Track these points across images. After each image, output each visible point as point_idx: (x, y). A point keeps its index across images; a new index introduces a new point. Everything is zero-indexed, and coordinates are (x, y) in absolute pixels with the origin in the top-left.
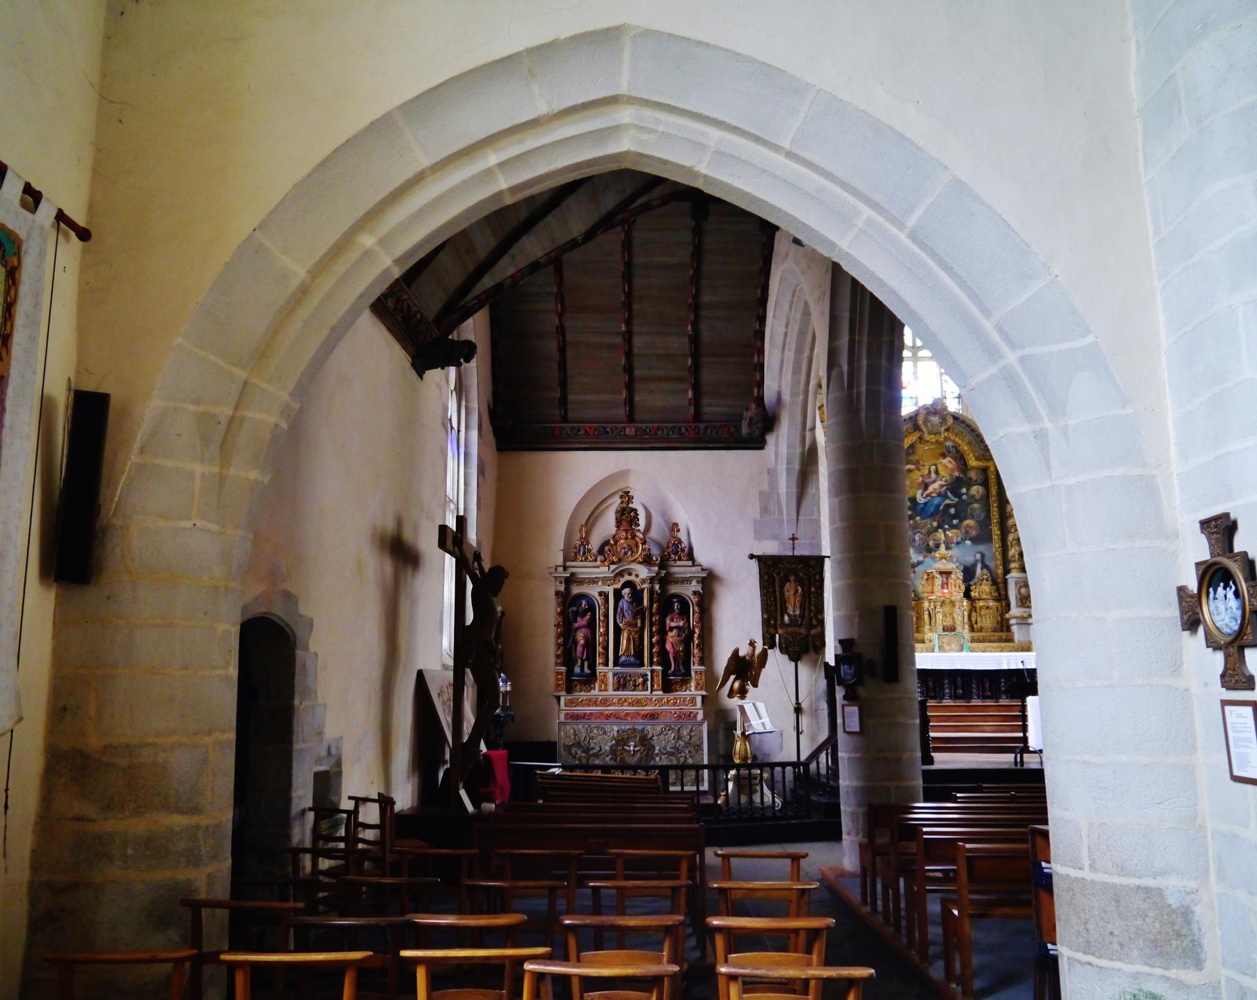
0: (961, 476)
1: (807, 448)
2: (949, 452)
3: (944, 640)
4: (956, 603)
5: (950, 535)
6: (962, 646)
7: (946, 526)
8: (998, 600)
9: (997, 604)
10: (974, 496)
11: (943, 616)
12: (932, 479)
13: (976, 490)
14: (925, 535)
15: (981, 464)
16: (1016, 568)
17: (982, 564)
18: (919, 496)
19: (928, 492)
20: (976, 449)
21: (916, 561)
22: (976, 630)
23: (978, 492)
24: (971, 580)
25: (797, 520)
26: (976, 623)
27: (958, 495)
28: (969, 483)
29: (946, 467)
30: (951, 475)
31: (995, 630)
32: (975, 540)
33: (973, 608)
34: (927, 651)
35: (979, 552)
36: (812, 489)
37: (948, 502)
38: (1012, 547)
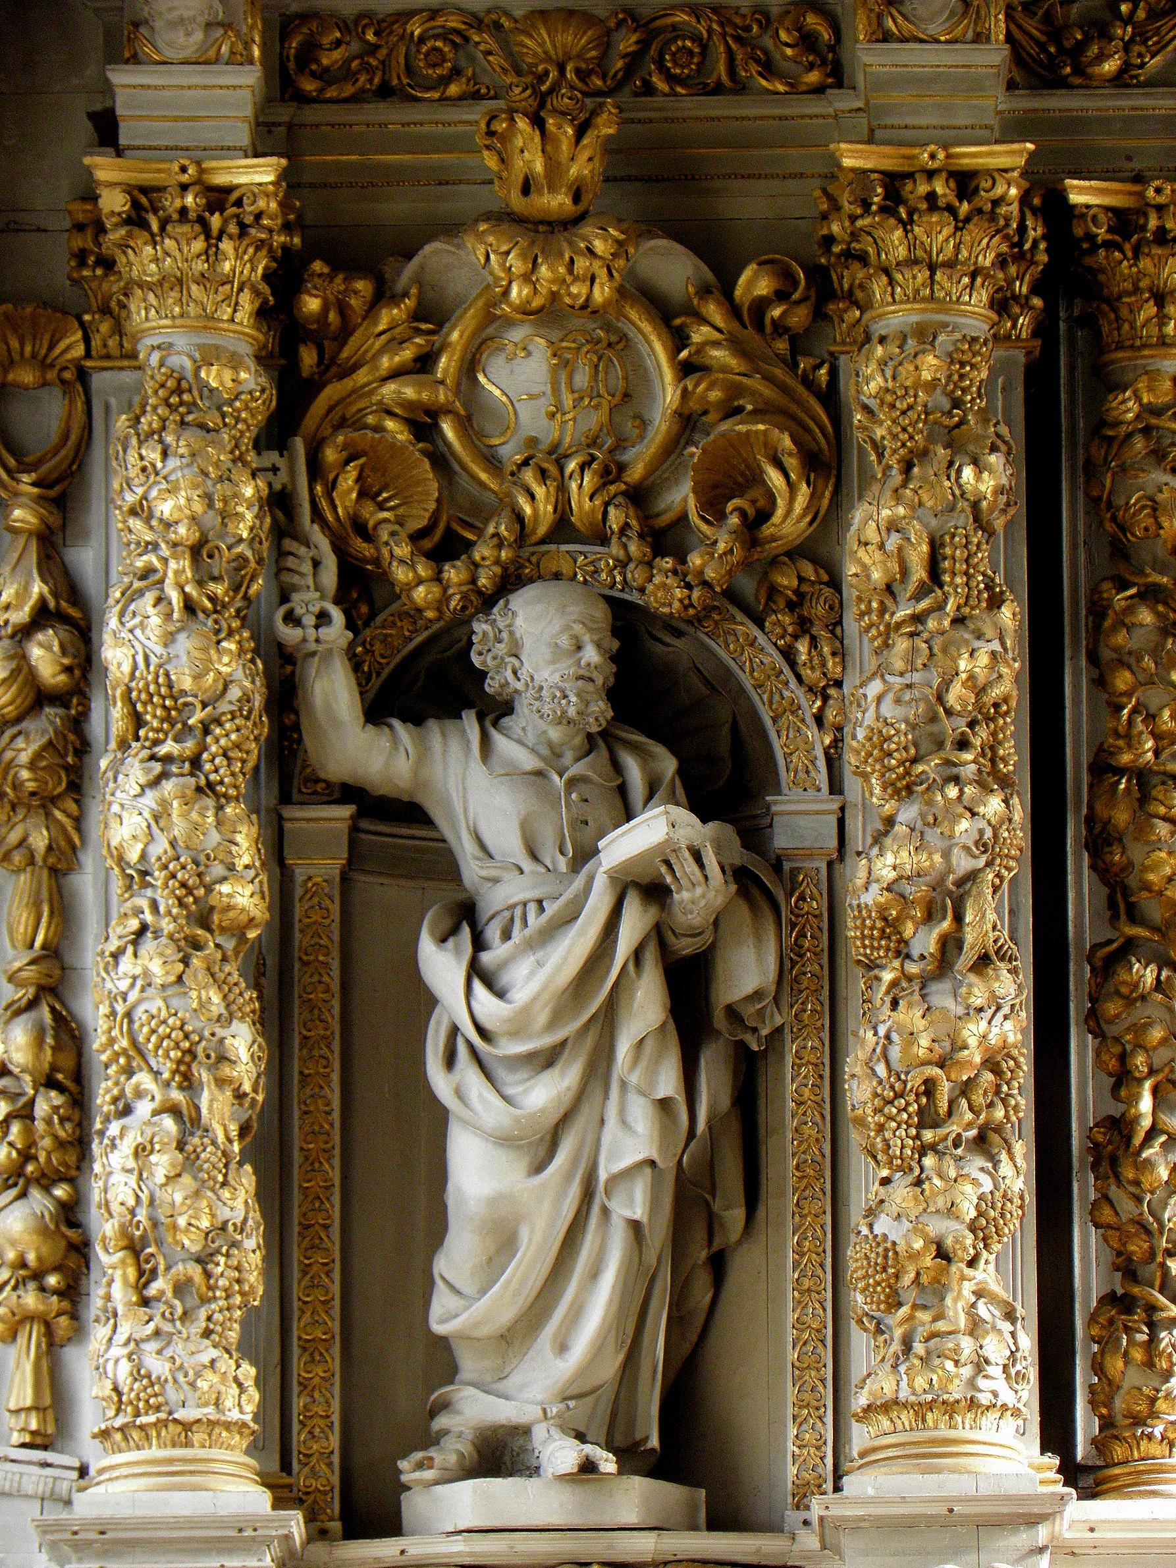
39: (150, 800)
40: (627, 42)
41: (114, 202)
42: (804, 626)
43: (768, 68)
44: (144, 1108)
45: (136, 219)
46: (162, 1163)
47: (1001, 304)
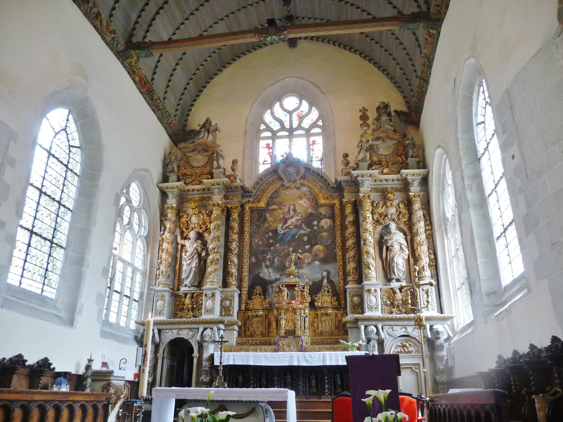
0: (313, 212)
2: (305, 195)
5: (300, 256)
7: (300, 251)
9: (336, 312)
11: (286, 322)
12: (291, 216)
14: (282, 258)
18: (279, 228)
19: (287, 225)
20: (326, 192)
21: (274, 278)
23: (327, 224)
26: (318, 329)
28: (319, 217)
29: (302, 206)
30: (306, 212)
35: (326, 271)
37: (302, 232)
38: (349, 263)
46: (163, 267)
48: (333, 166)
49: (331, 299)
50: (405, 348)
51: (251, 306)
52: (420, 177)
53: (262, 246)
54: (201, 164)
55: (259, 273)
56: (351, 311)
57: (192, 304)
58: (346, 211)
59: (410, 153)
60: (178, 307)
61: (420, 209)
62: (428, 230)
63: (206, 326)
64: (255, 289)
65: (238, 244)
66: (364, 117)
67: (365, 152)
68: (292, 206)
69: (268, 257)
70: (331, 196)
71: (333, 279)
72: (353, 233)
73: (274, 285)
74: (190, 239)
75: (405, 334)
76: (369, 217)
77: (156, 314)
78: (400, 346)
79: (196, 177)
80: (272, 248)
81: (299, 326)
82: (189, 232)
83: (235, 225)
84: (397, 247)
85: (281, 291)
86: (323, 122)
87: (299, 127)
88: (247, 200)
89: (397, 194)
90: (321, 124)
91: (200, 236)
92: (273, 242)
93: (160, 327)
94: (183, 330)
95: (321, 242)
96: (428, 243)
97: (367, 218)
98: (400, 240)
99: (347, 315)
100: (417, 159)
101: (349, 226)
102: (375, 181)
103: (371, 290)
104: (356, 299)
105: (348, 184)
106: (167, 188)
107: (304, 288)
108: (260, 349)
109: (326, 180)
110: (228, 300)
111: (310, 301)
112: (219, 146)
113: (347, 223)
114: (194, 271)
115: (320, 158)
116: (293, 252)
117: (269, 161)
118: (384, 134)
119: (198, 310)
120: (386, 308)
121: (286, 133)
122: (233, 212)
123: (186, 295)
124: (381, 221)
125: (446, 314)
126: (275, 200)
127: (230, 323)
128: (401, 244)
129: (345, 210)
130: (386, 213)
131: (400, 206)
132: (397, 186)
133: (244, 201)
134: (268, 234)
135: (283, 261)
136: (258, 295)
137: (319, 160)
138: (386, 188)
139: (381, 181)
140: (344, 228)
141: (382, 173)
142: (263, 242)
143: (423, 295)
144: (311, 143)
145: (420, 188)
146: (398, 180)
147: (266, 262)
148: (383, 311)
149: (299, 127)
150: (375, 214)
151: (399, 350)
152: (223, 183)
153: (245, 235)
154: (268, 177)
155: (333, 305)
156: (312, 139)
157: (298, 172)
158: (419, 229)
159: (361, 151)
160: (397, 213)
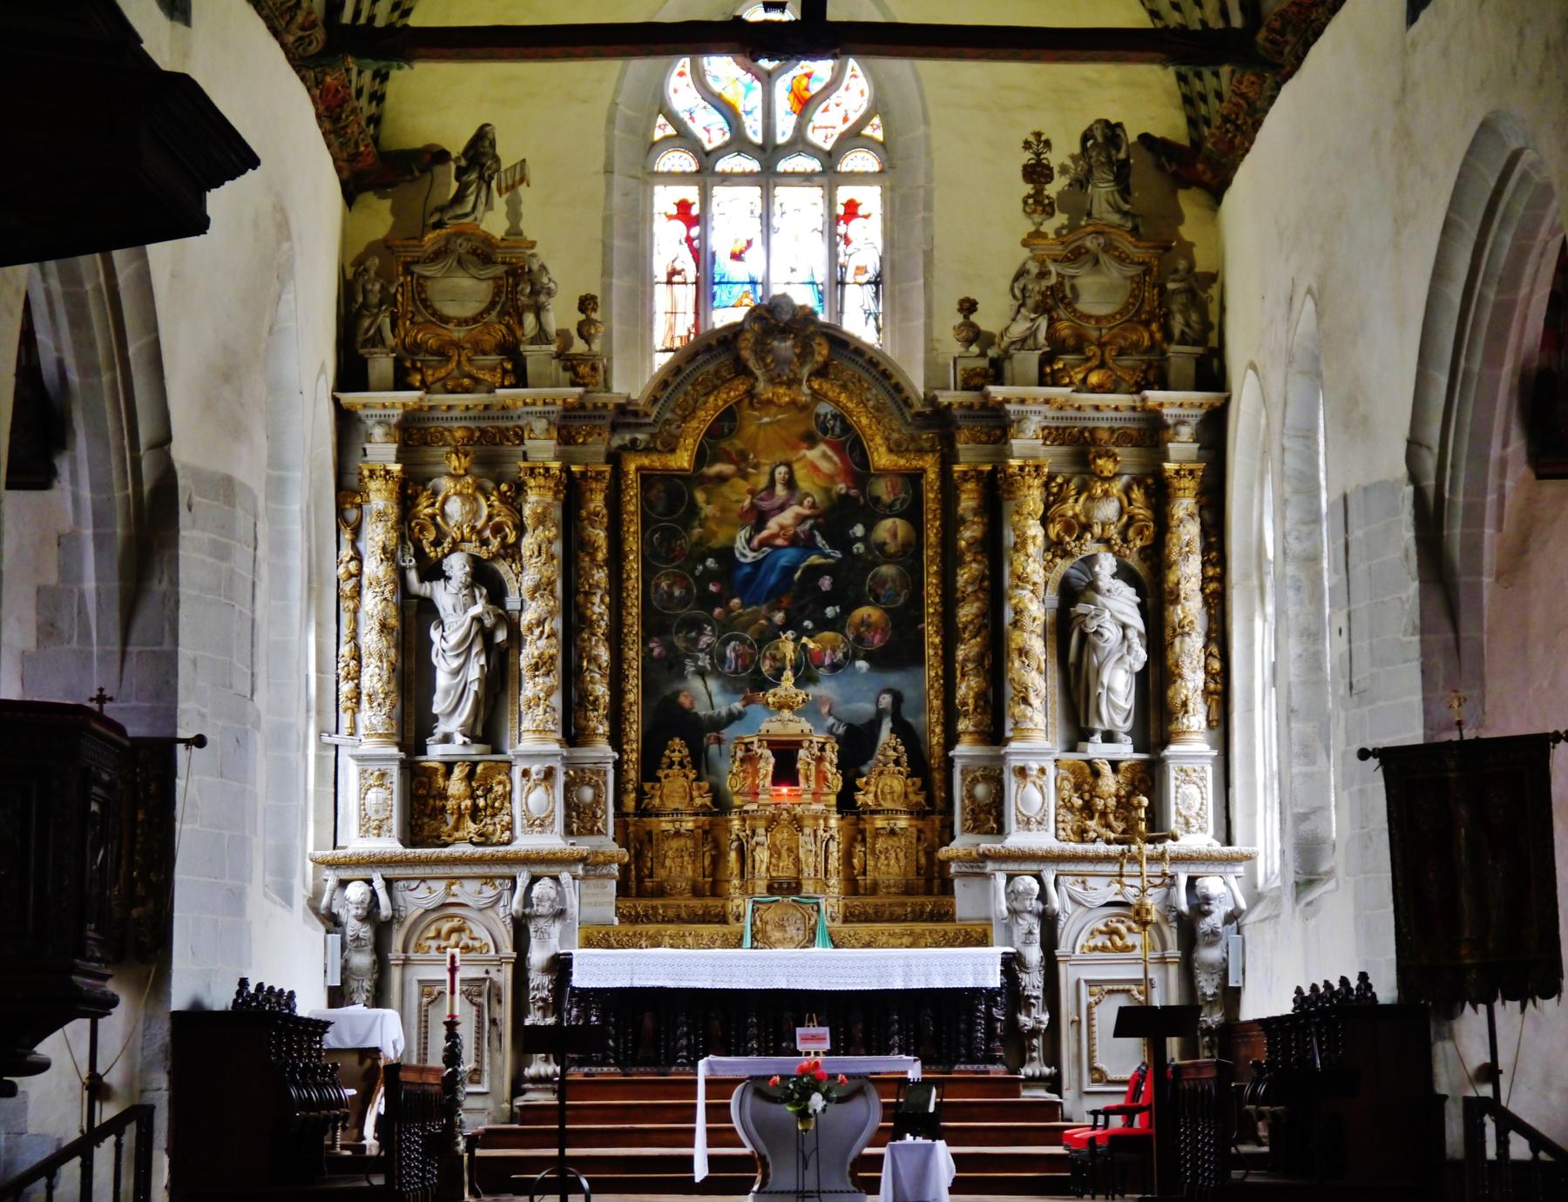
0: (853, 492)
1: (146, 488)
2: (825, 431)
3: (768, 916)
4: (806, 822)
5: (811, 645)
6: (813, 931)
7: (808, 624)
8: (916, 813)
9: (920, 824)
10: (885, 544)
11: (771, 856)
12: (777, 502)
13: (890, 530)
14: (751, 646)
15: (902, 462)
16: (970, 733)
17: (893, 721)
18: (740, 544)
19: (765, 533)
20: (896, 424)
21: (724, 712)
22: (862, 891)
23: (895, 535)
24: (864, 762)
25: (124, 654)
26: (864, 873)
27: (841, 540)
28: (872, 512)
29: (815, 468)
30: (827, 491)
31: (908, 890)
32: (882, 660)
33: (856, 836)
34: (726, 944)
36: (160, 582)
37: (814, 559)
38: (963, 675)
39: (373, 602)
40: (477, 434)
41: (366, 473)
42: (514, 561)
43: (508, 440)
44: (372, 666)
45: (371, 477)
46: (376, 678)
47: (556, 493)
48: (919, 323)
49: (906, 785)
50: (1116, 938)
51: (657, 801)
52: (1203, 411)
53: (683, 602)
54: (471, 309)
55: (677, 693)
56: (968, 824)
57: (473, 797)
58: (963, 505)
59: (1177, 324)
60: (426, 804)
61: (1191, 515)
62: (1212, 579)
63: (538, 870)
64: (665, 747)
65: (607, 599)
66: (1037, 173)
67: (1033, 316)
68: (782, 470)
69: (705, 640)
70: (912, 439)
71: (910, 720)
72: (982, 581)
73: (726, 733)
74: (448, 579)
75: (1119, 898)
76: (1034, 537)
77: (367, 831)
78: (1101, 932)
79: (459, 362)
80: (717, 611)
81: (812, 869)
82: (446, 556)
83: (600, 536)
84: (1112, 634)
85: (750, 759)
86: (886, 126)
87: (799, 143)
88: (628, 437)
89: (1125, 454)
90: (879, 135)
91: (484, 578)
92: (721, 590)
93: (391, 873)
94: (465, 882)
95: (877, 598)
96: (1209, 621)
97: (1030, 541)
98: (1123, 613)
99: (952, 838)
100: (1199, 350)
101: (968, 558)
102: (1061, 408)
103: (1031, 769)
104: (980, 790)
105: (971, 413)
106: (365, 406)
107: (822, 749)
108: (696, 936)
109: (898, 388)
110: (588, 784)
111: (840, 788)
112: (533, 244)
113: (963, 543)
114: (476, 692)
115: (870, 275)
116: (784, 628)
117: (691, 273)
118: (1102, 240)
119: (493, 816)
120: (1069, 817)
121: (752, 165)
122: (591, 490)
123: (449, 767)
124: (1072, 545)
125: (1238, 847)
126: (725, 445)
127: (601, 858)
128: (1124, 627)
129: (957, 503)
130: (1087, 516)
131: (1134, 496)
132: (1128, 425)
133: (617, 441)
134: (703, 561)
135: (753, 656)
136: (676, 767)
137: (869, 283)
138: (1093, 431)
139: (1079, 408)
140: (950, 559)
141: (1084, 386)
142: (688, 589)
143: (1177, 787)
144: (840, 210)
145: (1197, 445)
146: (1133, 408)
147: (697, 659)
148: (1061, 825)
149: (799, 143)
150: (1053, 521)
151: (1100, 944)
152: (565, 400)
153: (628, 567)
154: (700, 359)
155: (908, 806)
156: (844, 194)
157: (805, 353)
158: (1183, 582)
159: (1023, 310)
160: (1119, 519)
